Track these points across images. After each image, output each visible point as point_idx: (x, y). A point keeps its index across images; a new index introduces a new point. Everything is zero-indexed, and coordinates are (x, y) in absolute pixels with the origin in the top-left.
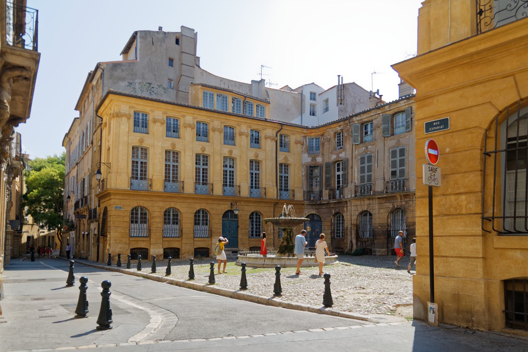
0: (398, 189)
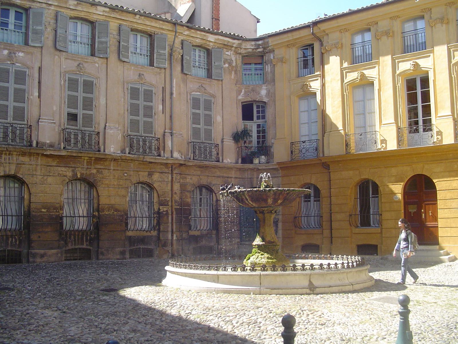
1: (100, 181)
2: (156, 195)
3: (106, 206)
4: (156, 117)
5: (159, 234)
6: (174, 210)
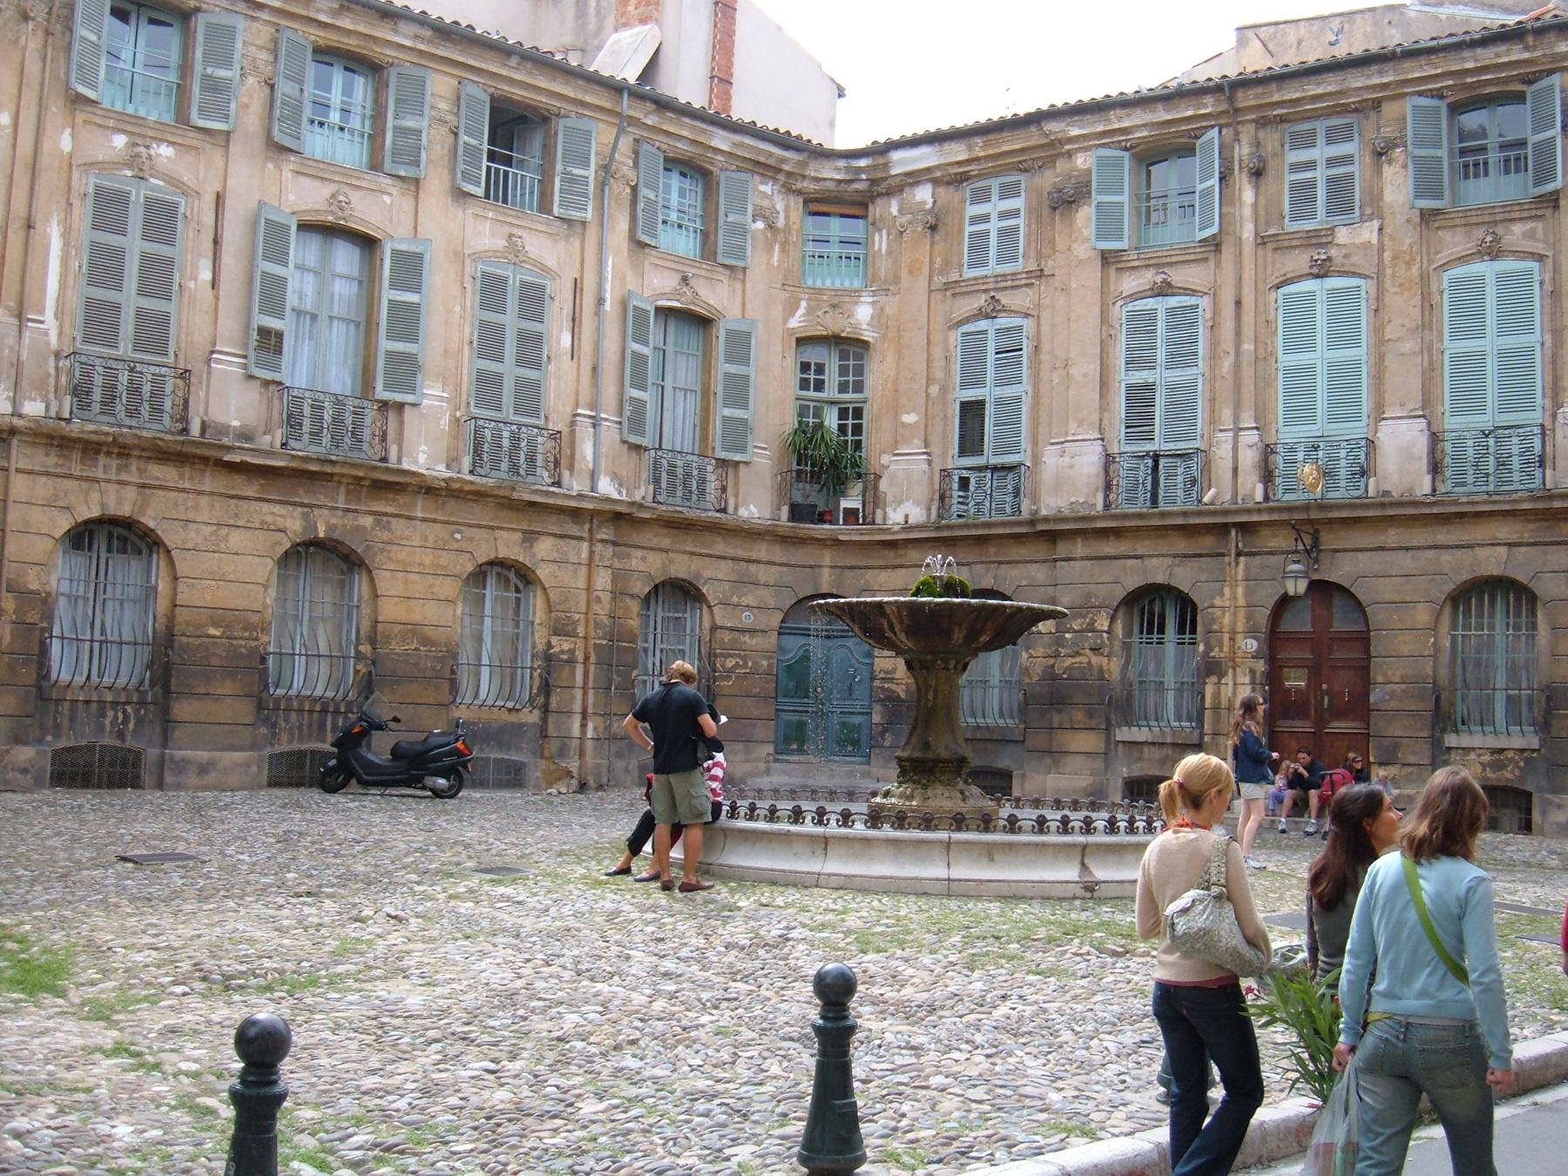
0: (326, 439)
1: (382, 551)
2: (539, 601)
3: (398, 628)
4: (552, 368)
5: (544, 719)
6: (591, 650)
